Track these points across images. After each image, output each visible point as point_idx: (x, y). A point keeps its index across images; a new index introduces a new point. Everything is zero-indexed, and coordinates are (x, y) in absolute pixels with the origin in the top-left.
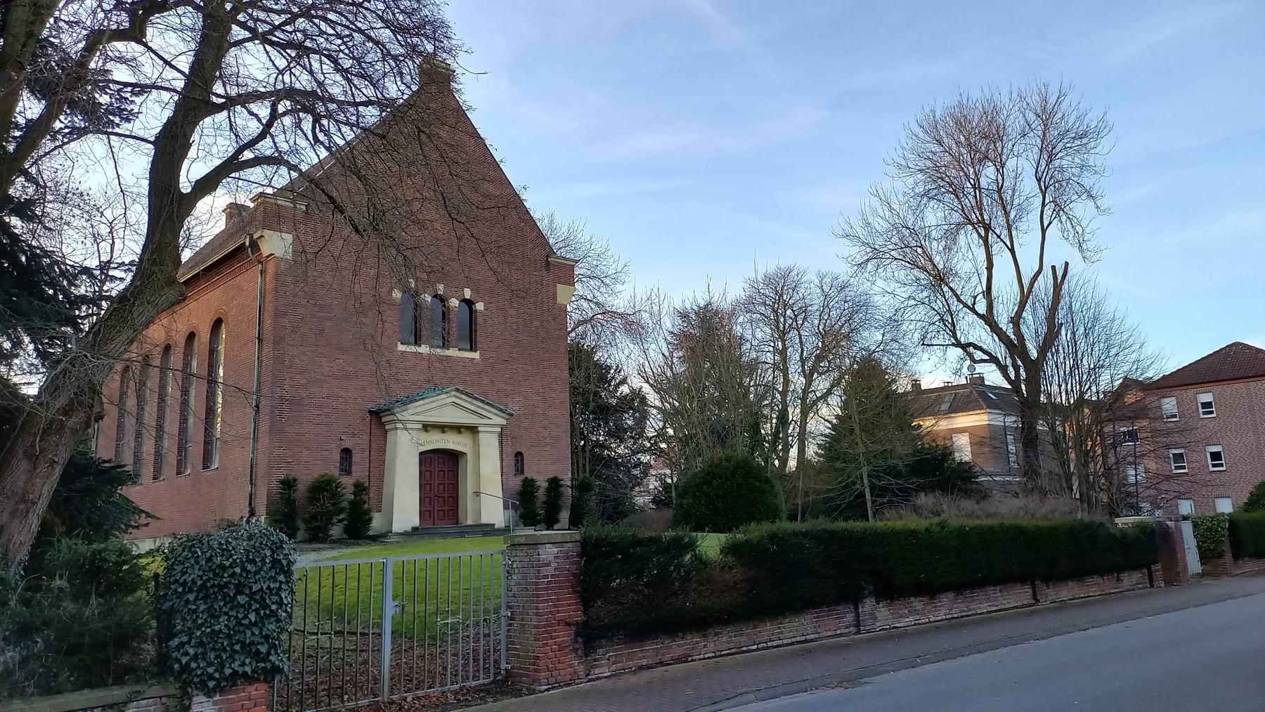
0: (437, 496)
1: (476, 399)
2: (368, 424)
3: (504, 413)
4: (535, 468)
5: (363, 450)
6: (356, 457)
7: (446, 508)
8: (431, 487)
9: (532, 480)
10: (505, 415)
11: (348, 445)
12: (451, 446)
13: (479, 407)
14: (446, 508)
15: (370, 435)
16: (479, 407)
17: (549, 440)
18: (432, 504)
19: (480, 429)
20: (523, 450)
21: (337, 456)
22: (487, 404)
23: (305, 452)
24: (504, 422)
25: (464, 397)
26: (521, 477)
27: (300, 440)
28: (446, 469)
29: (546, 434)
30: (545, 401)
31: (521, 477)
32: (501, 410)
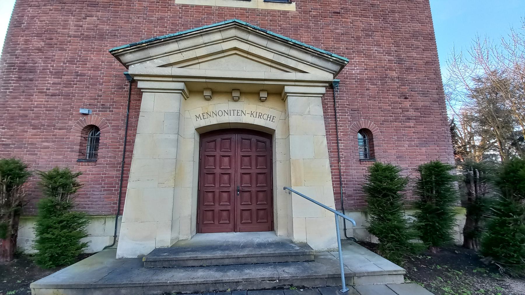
0: (238, 191)
1: (273, 39)
2: (126, 94)
3: (327, 60)
4: (394, 152)
5: (116, 128)
6: (105, 138)
7: (254, 207)
8: (230, 179)
9: (389, 169)
10: (330, 66)
11: (92, 120)
12: (247, 119)
13: (282, 54)
14: (254, 207)
15: (129, 109)
16: (282, 54)
17: (411, 113)
18: (232, 200)
19: (287, 89)
20: (371, 126)
21: (76, 136)
22: (294, 46)
23: (31, 131)
24: (329, 77)
25: (252, 38)
26: (370, 164)
27: (27, 116)
28: (253, 154)
29: (407, 104)
30: (400, 61)
31: (370, 164)
32: (320, 56)
